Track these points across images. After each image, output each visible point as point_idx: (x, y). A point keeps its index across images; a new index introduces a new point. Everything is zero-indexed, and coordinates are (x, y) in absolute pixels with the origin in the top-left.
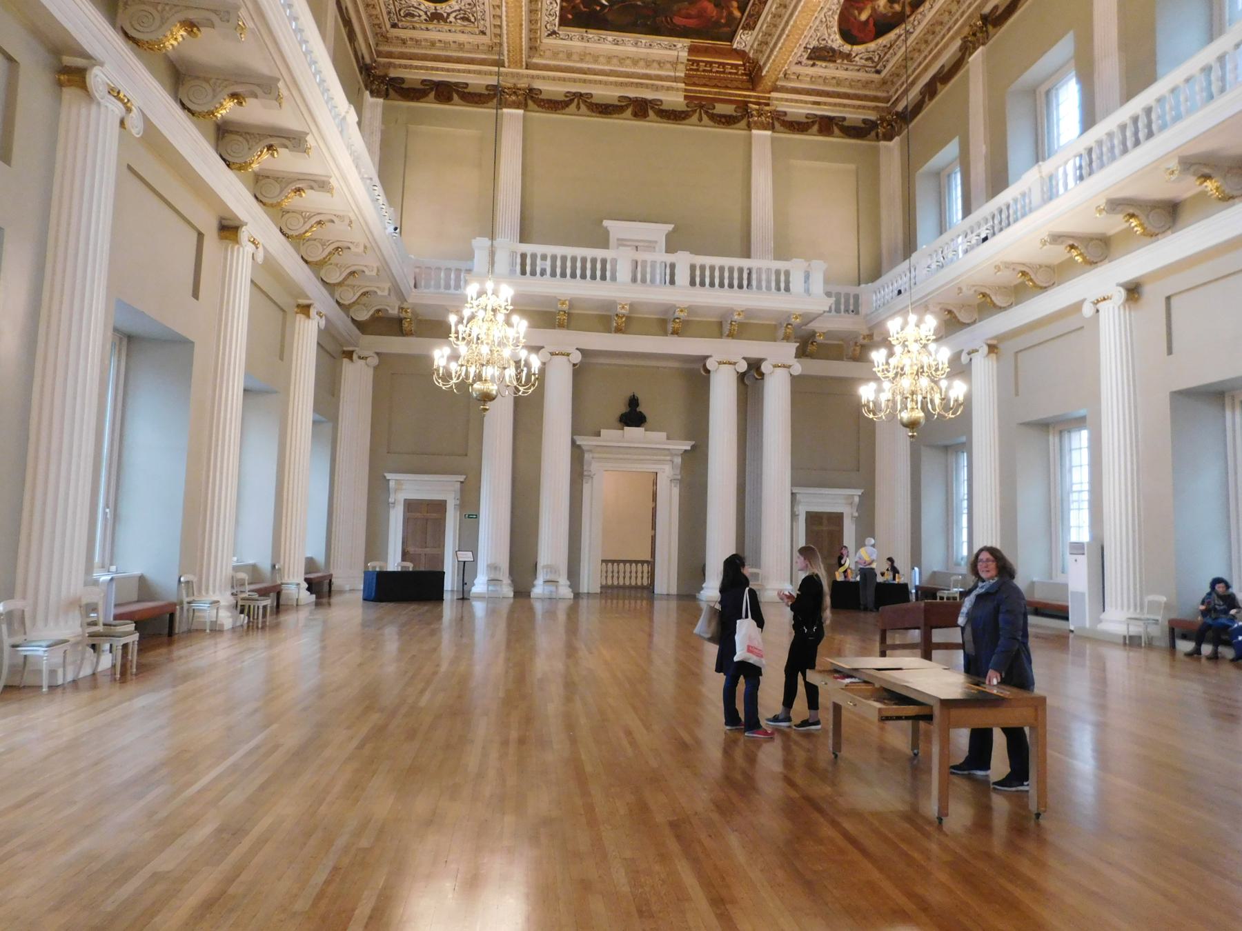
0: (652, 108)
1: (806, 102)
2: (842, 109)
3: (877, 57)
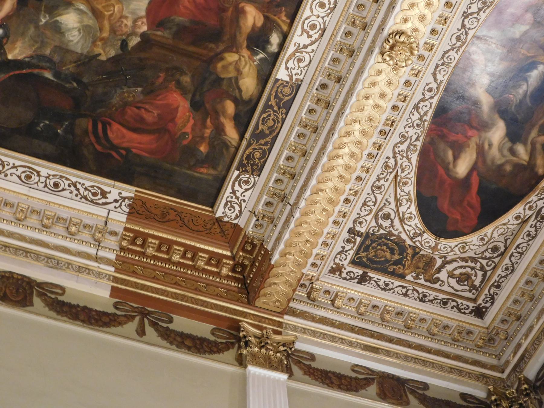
0: (41, 295)
1: (351, 344)
2: (419, 367)
3: (480, 274)
